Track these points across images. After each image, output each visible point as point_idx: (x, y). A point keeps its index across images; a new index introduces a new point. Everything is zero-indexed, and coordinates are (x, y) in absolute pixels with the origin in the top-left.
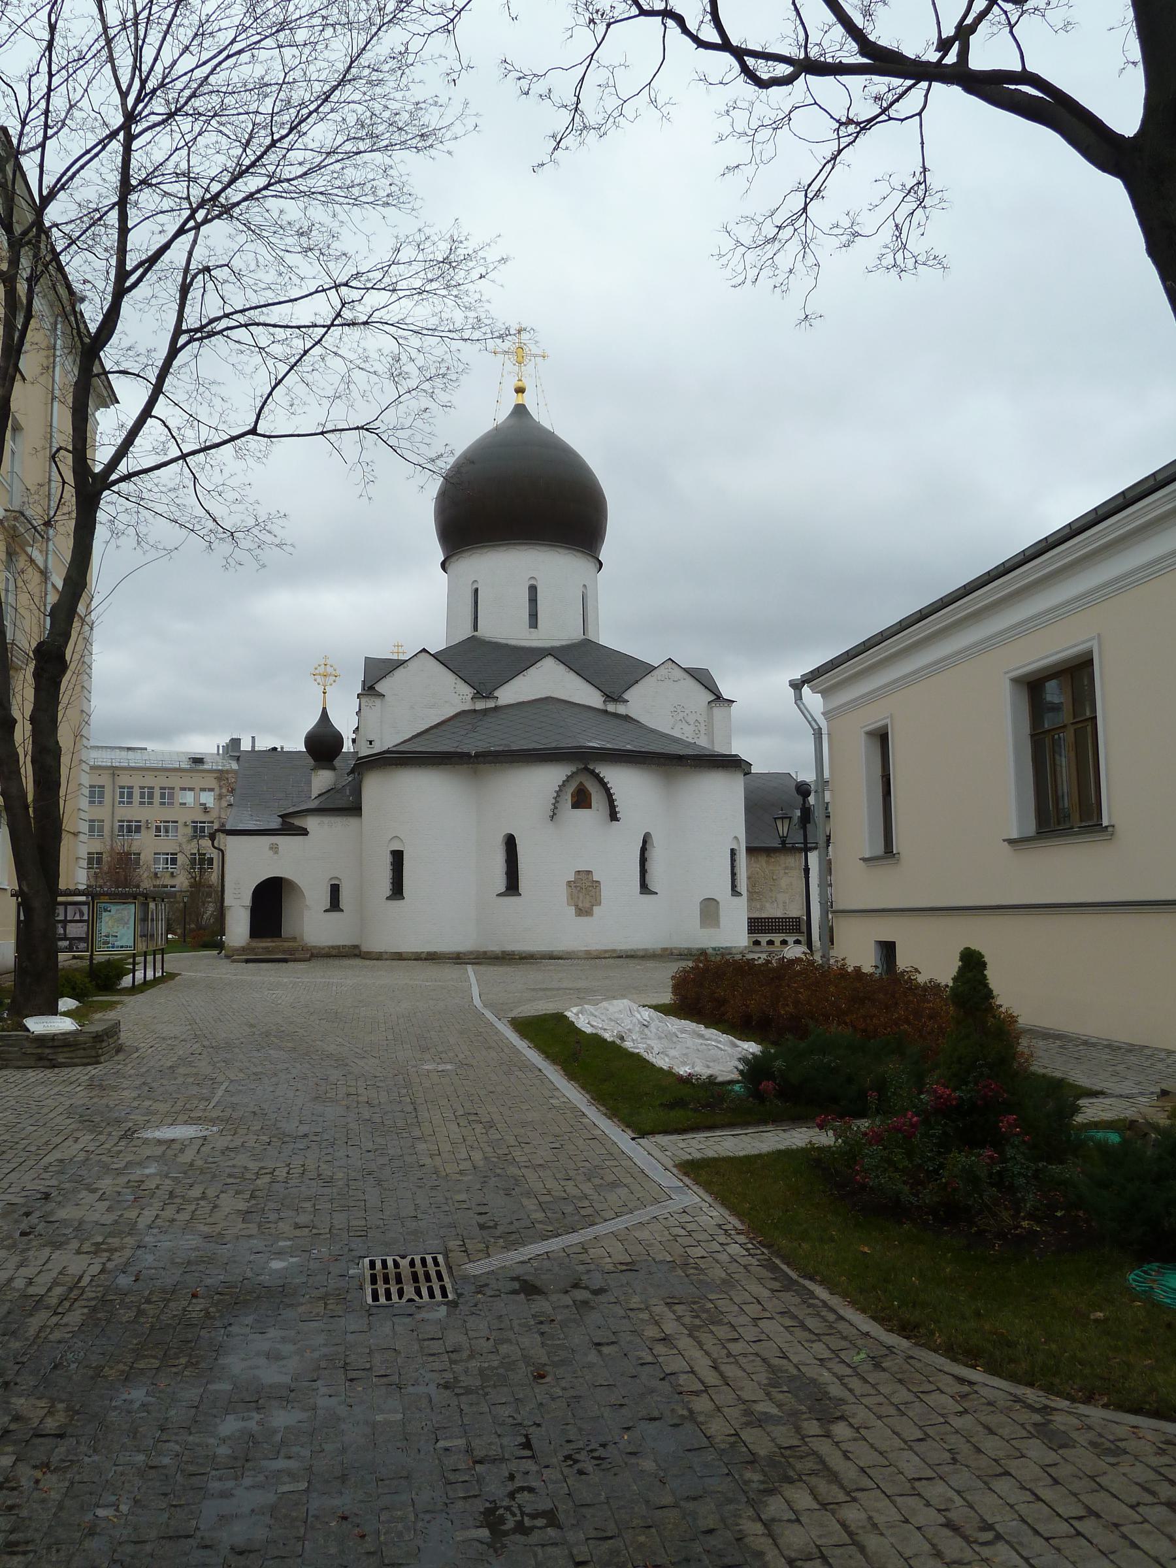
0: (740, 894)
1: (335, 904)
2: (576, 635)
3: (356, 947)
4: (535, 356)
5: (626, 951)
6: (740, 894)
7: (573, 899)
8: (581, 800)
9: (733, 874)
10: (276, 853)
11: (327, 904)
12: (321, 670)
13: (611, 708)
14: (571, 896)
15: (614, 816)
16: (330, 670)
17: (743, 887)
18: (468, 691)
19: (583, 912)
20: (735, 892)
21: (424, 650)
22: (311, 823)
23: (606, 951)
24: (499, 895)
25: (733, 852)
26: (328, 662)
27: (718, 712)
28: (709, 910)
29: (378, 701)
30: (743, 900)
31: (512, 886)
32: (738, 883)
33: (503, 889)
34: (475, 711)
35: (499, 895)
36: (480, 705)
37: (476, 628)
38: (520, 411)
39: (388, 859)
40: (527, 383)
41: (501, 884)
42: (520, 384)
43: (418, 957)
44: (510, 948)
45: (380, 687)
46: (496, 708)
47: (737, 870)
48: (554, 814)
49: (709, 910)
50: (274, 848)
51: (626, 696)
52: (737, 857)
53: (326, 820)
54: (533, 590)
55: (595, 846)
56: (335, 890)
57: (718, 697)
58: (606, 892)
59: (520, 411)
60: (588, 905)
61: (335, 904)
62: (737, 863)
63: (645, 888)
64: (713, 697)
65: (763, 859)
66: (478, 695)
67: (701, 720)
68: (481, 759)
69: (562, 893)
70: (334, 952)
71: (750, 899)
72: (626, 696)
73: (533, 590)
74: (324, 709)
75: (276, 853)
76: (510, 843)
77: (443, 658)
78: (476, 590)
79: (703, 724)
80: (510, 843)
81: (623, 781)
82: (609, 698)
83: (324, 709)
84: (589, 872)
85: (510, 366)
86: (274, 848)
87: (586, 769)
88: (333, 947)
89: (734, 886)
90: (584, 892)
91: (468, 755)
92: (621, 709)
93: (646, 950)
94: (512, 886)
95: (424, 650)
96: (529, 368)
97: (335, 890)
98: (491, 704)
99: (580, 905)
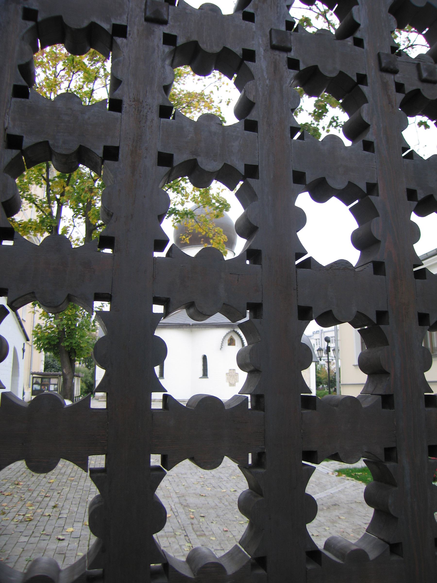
14: (228, 379)
24: (200, 378)
31: (205, 374)
35: (200, 378)
41: (201, 373)
48: (222, 347)
60: (233, 382)
68: (194, 326)
69: (225, 377)
76: (205, 358)
80: (205, 358)
87: (234, 331)
91: (189, 325)
94: (205, 374)
99: (231, 382)
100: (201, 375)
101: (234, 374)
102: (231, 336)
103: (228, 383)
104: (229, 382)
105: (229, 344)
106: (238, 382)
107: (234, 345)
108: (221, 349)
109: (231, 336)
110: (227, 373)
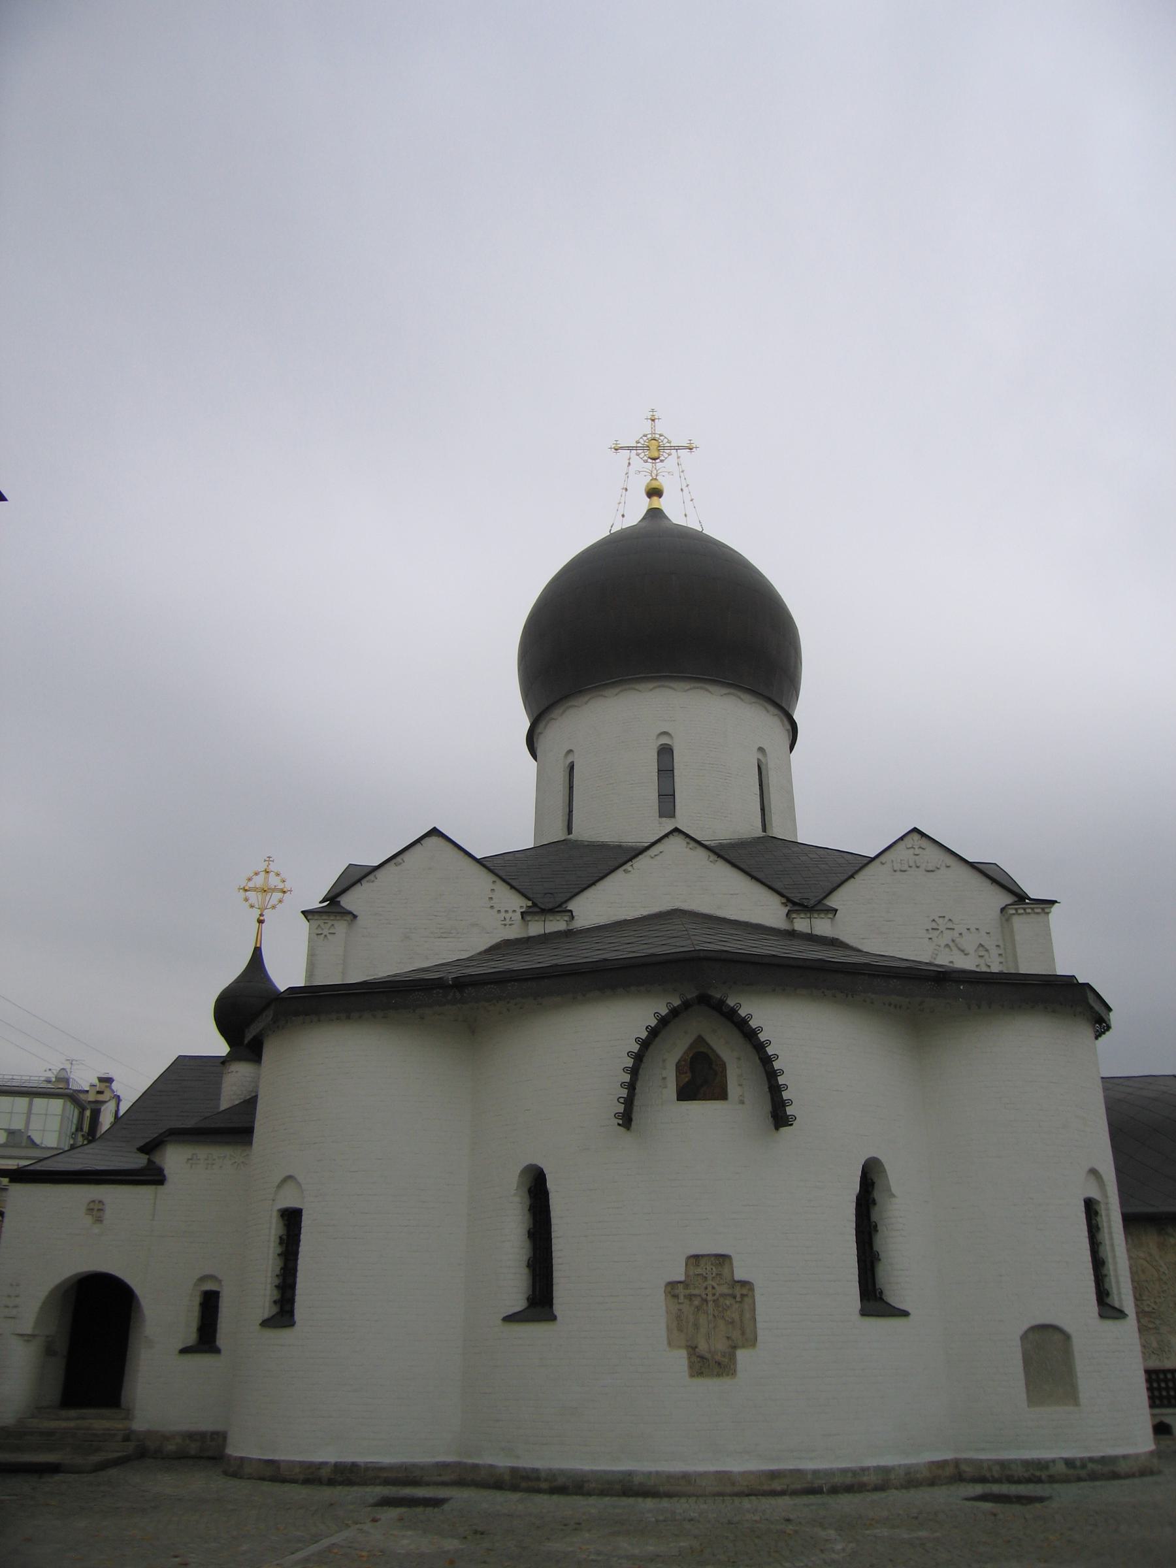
0: (1119, 1314)
1: (206, 1337)
2: (747, 826)
3: (220, 1438)
4: (677, 448)
5: (829, 1473)
6: (1119, 1314)
7: (682, 1328)
8: (701, 1081)
9: (1098, 1263)
10: (99, 1220)
11: (191, 1337)
12: (259, 881)
13: (801, 924)
14: (678, 1323)
15: (780, 1116)
16: (274, 881)
17: (1124, 1294)
18: (516, 903)
19: (710, 1364)
20: (1107, 1308)
21: (434, 832)
22: (174, 1159)
23: (774, 1475)
24: (510, 1319)
25: (1090, 1207)
26: (272, 867)
27: (1022, 924)
28: (1047, 1357)
29: (341, 926)
30: (1129, 1328)
32: (1112, 1284)
33: (518, 1303)
34: (529, 939)
35: (510, 1319)
36: (536, 928)
37: (570, 831)
38: (655, 514)
39: (272, 1229)
40: (664, 482)
41: (513, 1290)
42: (655, 484)
43: (312, 1476)
44: (529, 1461)
45: (347, 901)
46: (568, 934)
47: (1106, 1252)
49: (1047, 1357)
50: (96, 1211)
51: (833, 902)
52: (1103, 1221)
53: (203, 1152)
54: (665, 753)
55: (744, 1192)
56: (210, 1303)
57: (1020, 897)
58: (768, 1309)
59: (655, 514)
60: (721, 1345)
61: (206, 1337)
62: (1104, 1236)
63: (873, 1298)
64: (1007, 899)
65: (1151, 1240)
66: (536, 910)
67: (989, 943)
70: (193, 1448)
71: (1142, 1329)
72: (833, 902)
73: (665, 753)
74: (257, 953)
75: (99, 1220)
76: (537, 1188)
77: (501, 868)
78: (571, 767)
79: (994, 952)
80: (537, 1188)
81: (802, 1035)
82: (796, 906)
83: (257, 953)
84: (723, 1259)
85: (638, 462)
86: (96, 1211)
88: (191, 1436)
89: (1102, 1294)
90: (712, 1309)
92: (822, 926)
93: (886, 1470)
95: (434, 832)
96: (669, 462)
97: (210, 1303)
98: (556, 925)
99: (703, 1347)
100: (515, 1295)
101: (725, 1289)
102: (700, 1040)
103: (683, 1353)
104: (692, 1349)
105: (686, 1093)
106: (751, 1341)
107: (722, 1095)
108: (626, 1119)
109: (700, 1040)
110: (672, 1285)
